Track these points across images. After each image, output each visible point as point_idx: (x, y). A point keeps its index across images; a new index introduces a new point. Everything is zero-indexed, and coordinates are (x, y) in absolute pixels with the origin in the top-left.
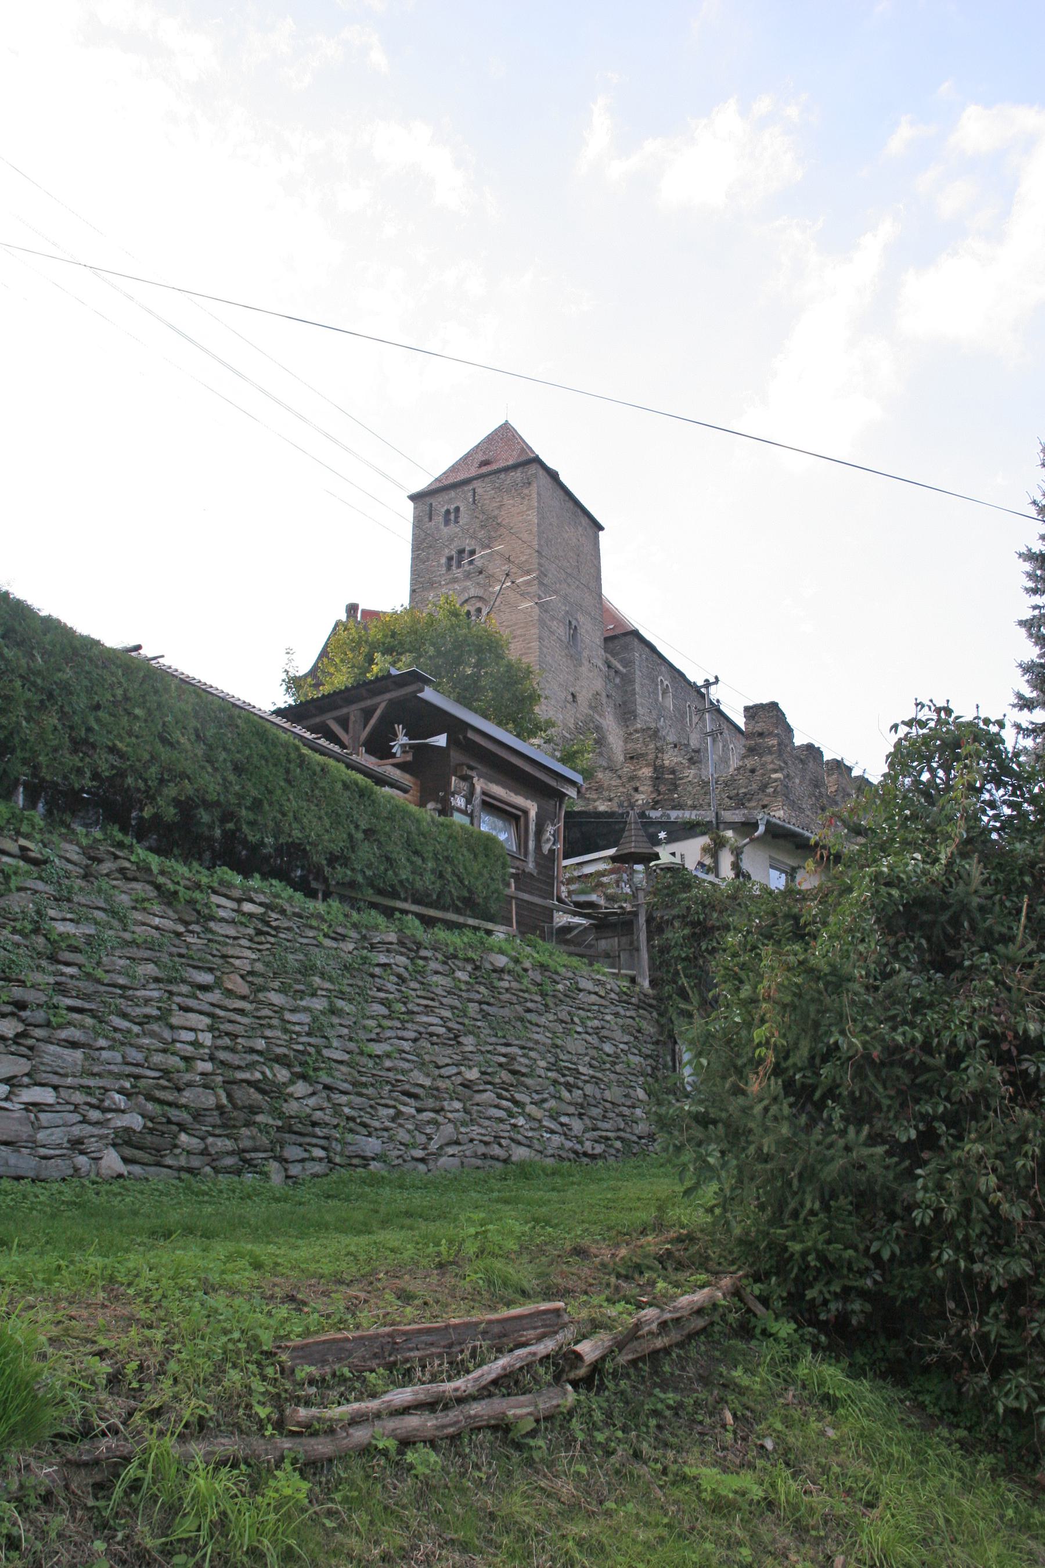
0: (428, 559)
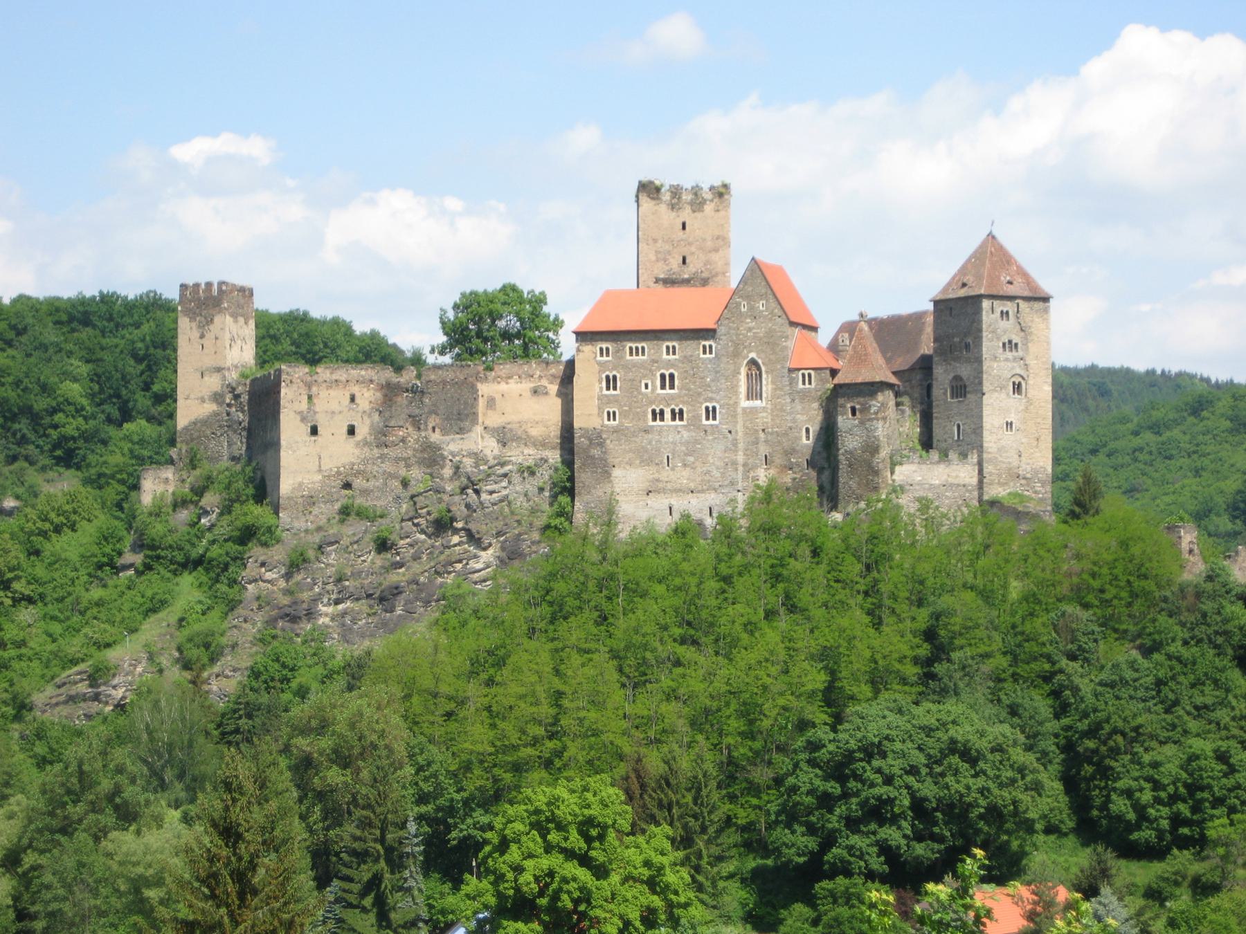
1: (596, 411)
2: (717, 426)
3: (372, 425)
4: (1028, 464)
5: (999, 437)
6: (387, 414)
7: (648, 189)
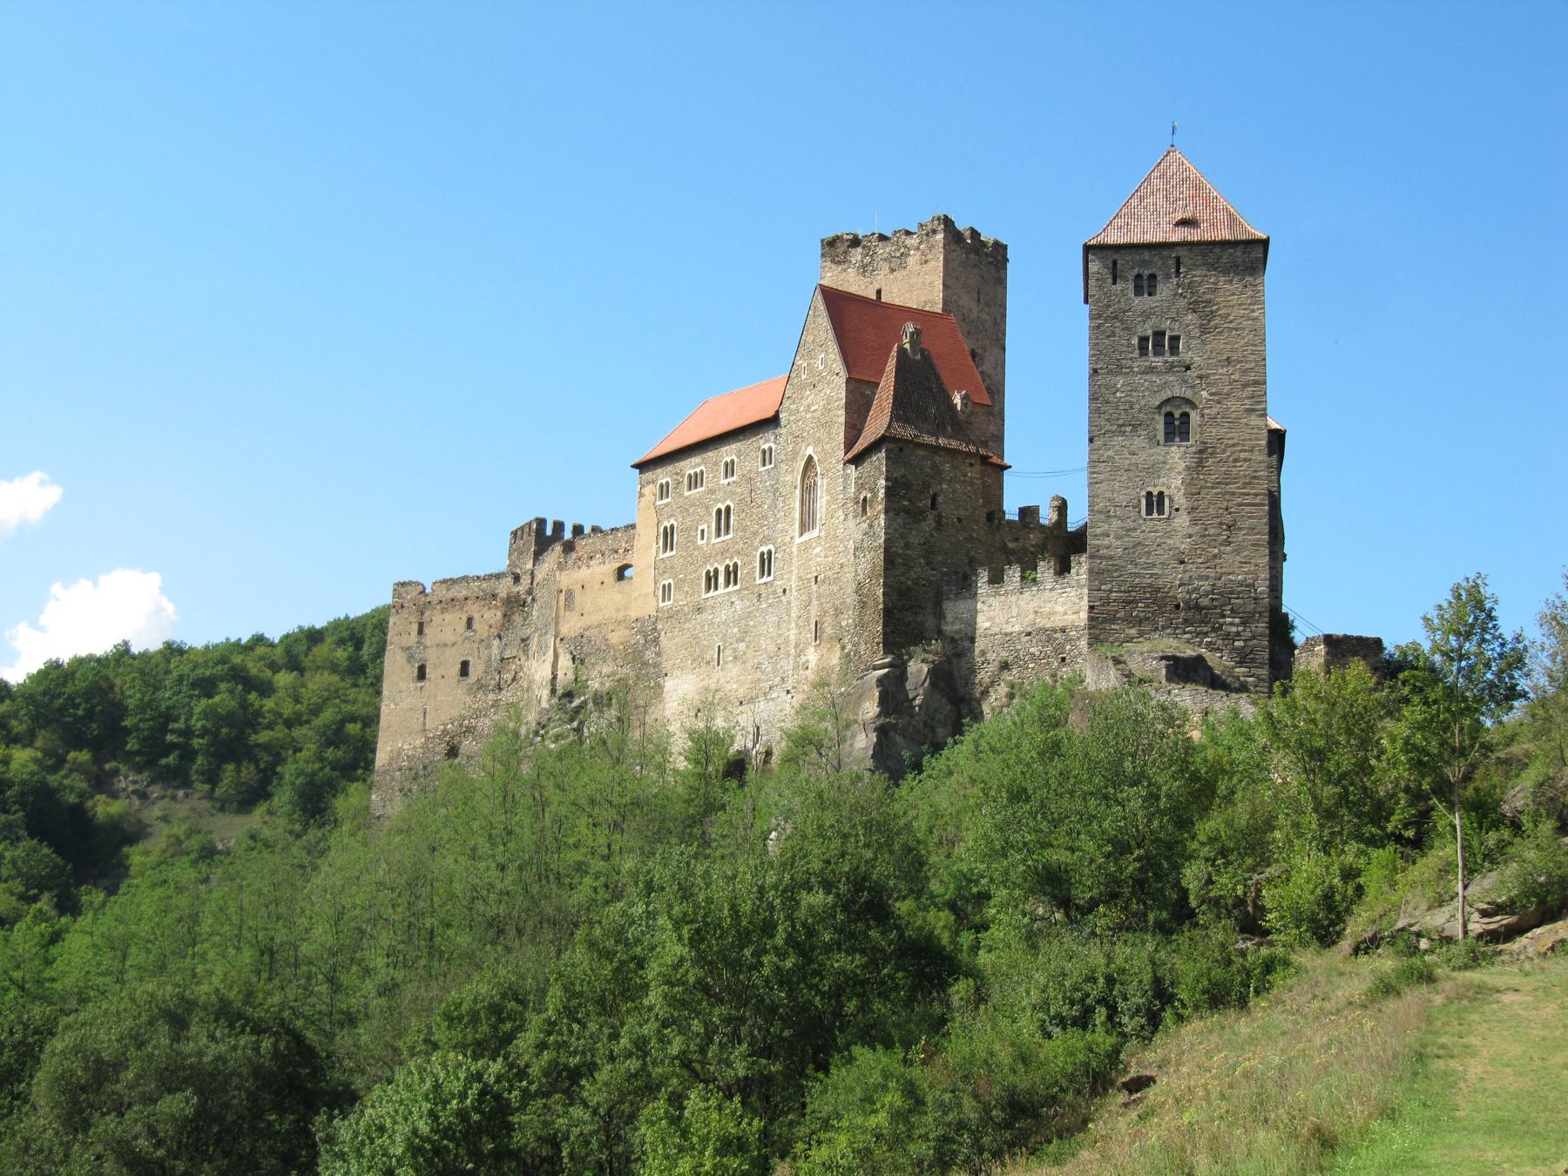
4: (1207, 578)
6: (504, 640)
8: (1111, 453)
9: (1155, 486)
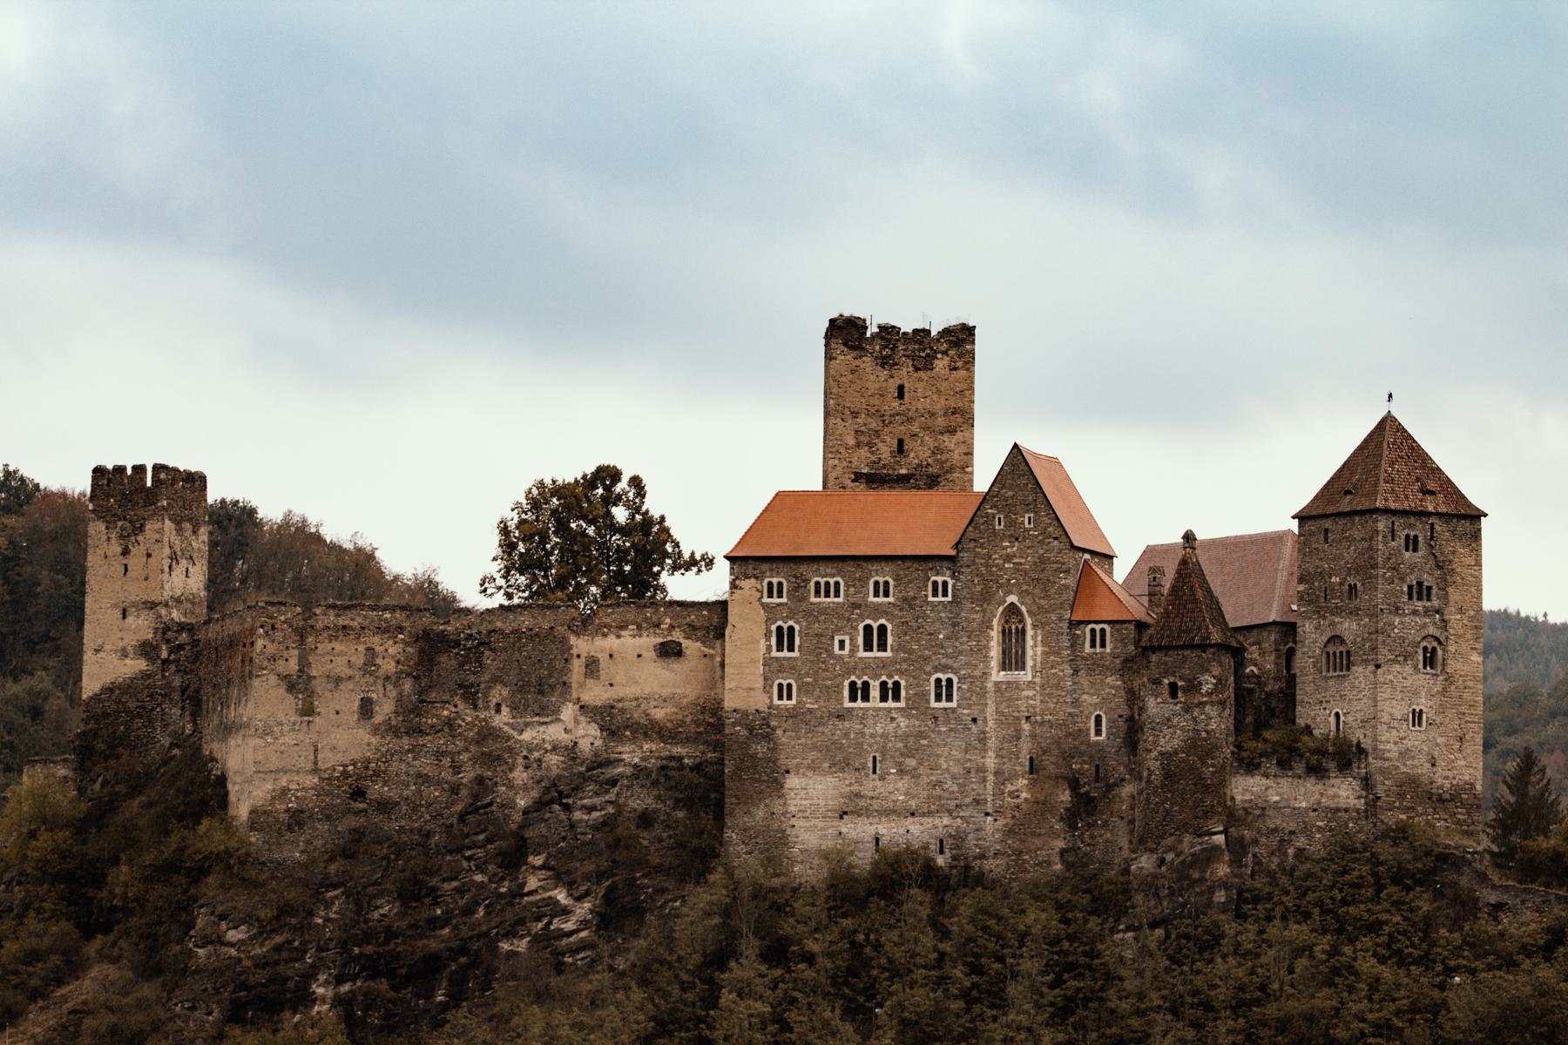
0: (1393, 582)
1: (760, 683)
2: (953, 710)
3: (399, 700)
5: (1402, 734)
7: (845, 332)
8: (1391, 677)
9: (1418, 704)
